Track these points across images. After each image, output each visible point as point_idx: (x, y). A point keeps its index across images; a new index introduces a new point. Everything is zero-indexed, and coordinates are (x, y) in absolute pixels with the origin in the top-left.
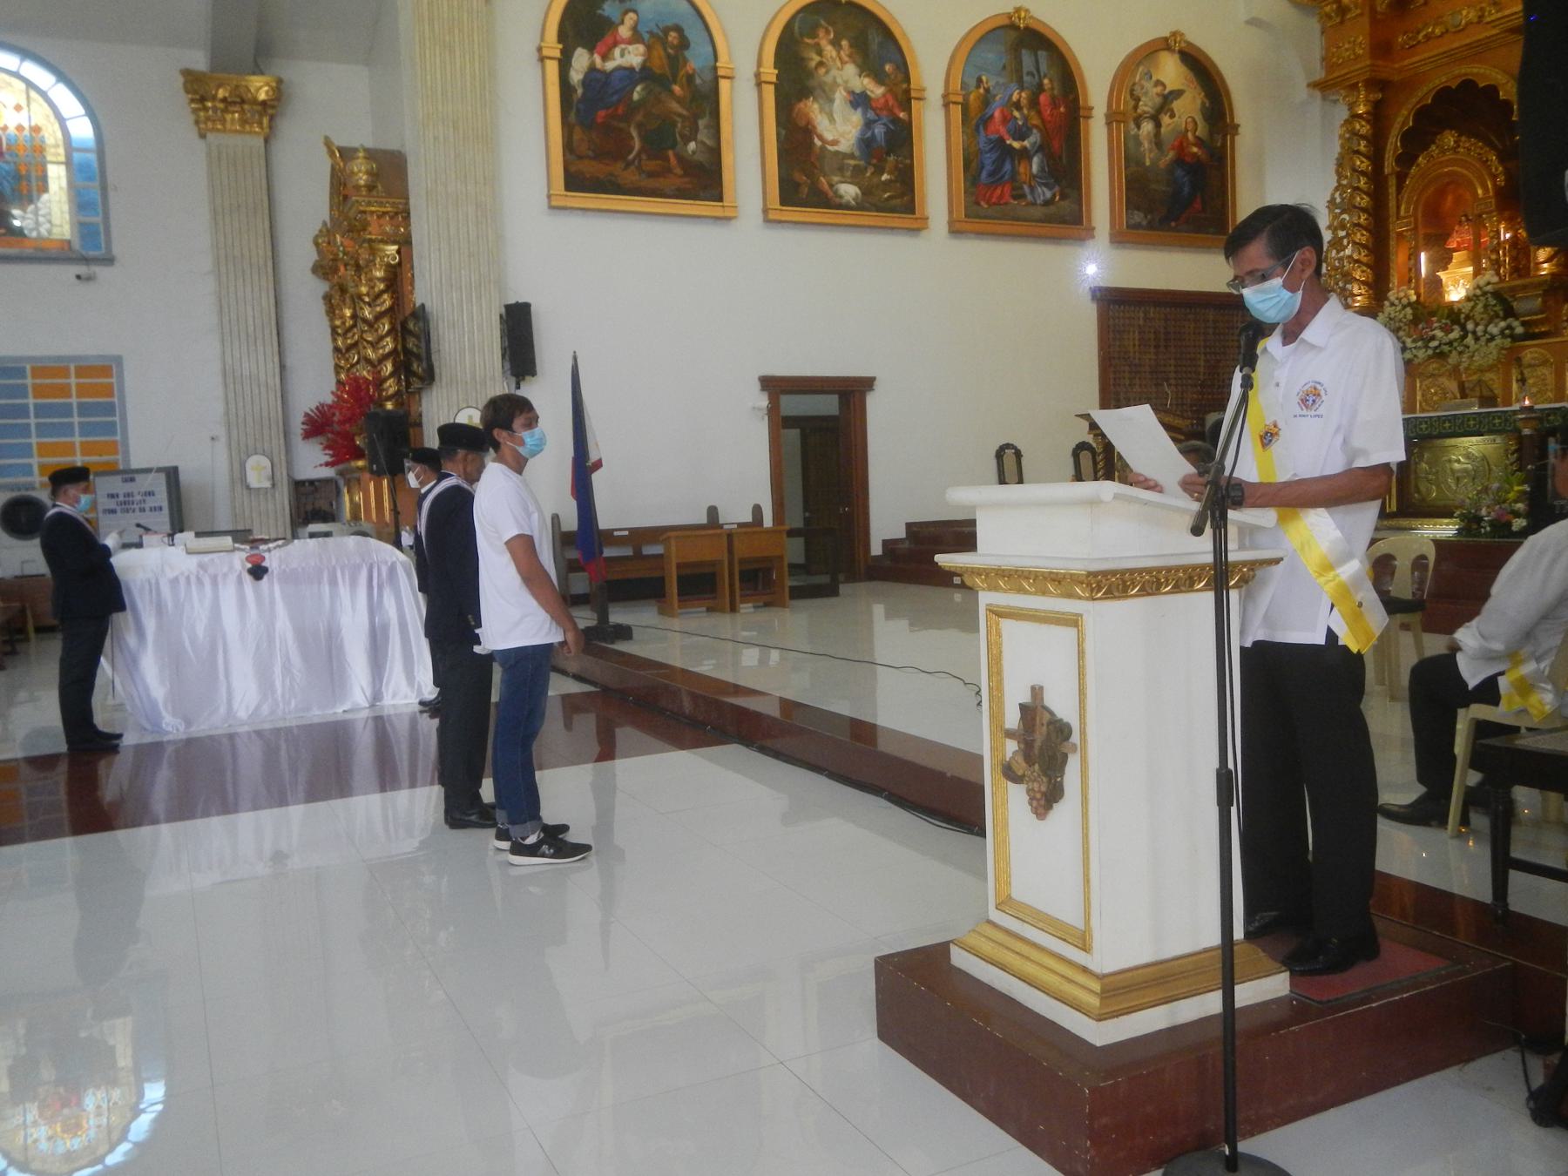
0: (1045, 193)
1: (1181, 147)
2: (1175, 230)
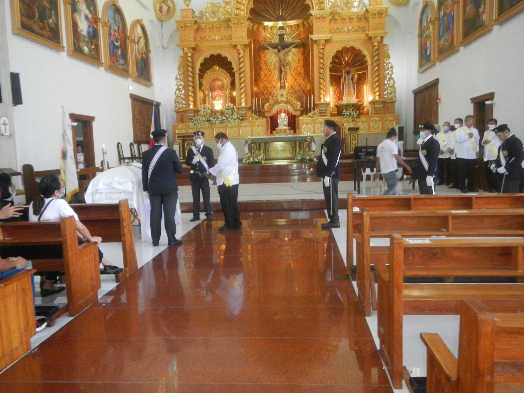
0: (122, 61)
1: (142, 54)
2: (142, 78)
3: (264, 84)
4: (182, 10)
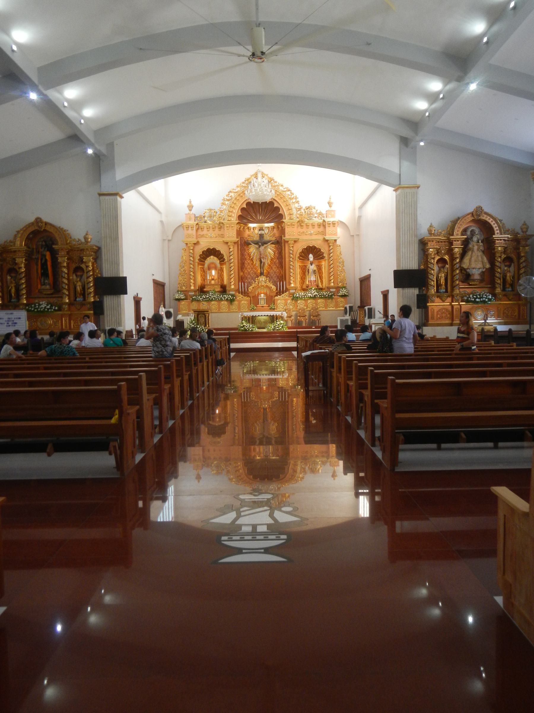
3: (248, 271)
4: (186, 214)
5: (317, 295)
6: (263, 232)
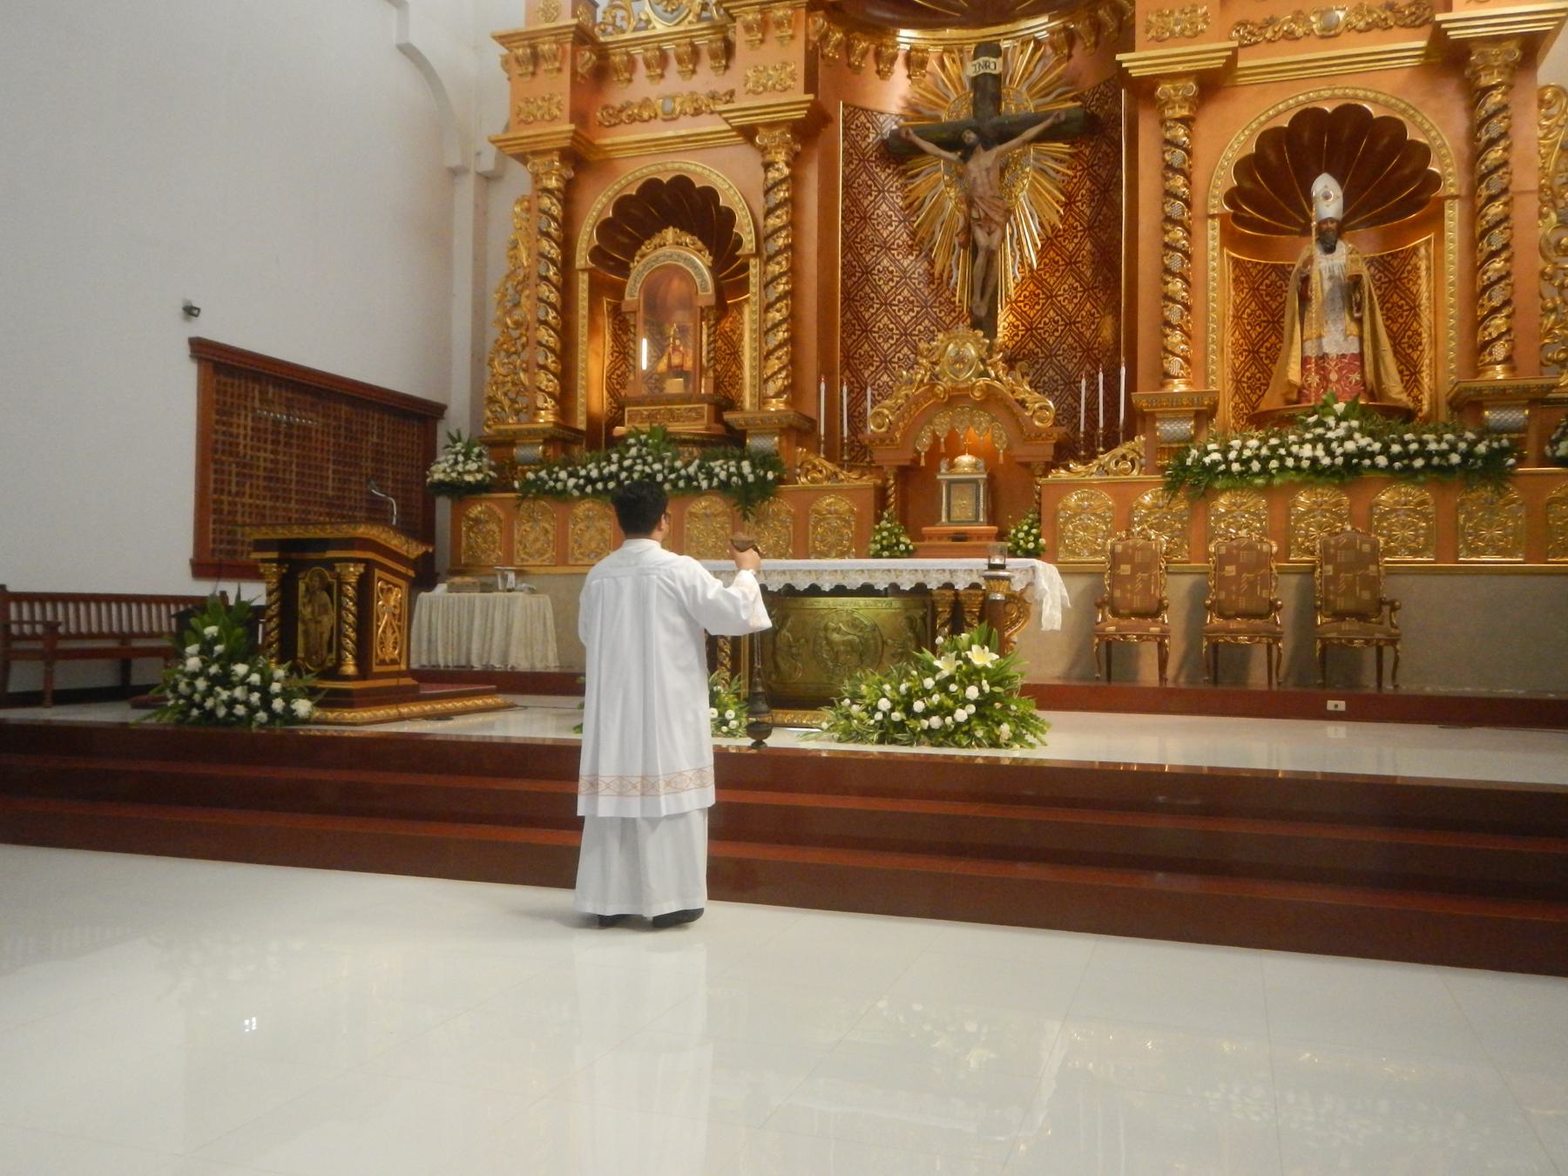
3: (896, 319)
5: (1372, 455)
6: (995, 65)
